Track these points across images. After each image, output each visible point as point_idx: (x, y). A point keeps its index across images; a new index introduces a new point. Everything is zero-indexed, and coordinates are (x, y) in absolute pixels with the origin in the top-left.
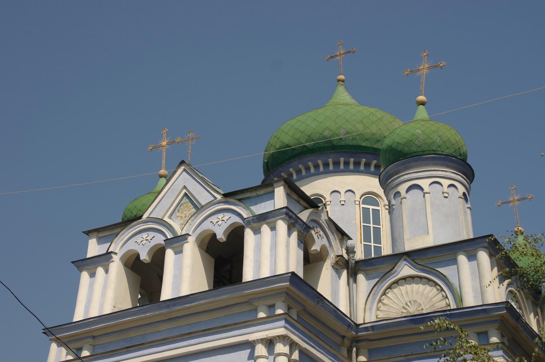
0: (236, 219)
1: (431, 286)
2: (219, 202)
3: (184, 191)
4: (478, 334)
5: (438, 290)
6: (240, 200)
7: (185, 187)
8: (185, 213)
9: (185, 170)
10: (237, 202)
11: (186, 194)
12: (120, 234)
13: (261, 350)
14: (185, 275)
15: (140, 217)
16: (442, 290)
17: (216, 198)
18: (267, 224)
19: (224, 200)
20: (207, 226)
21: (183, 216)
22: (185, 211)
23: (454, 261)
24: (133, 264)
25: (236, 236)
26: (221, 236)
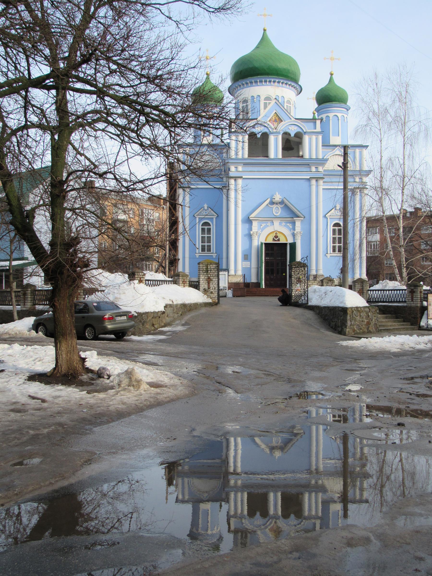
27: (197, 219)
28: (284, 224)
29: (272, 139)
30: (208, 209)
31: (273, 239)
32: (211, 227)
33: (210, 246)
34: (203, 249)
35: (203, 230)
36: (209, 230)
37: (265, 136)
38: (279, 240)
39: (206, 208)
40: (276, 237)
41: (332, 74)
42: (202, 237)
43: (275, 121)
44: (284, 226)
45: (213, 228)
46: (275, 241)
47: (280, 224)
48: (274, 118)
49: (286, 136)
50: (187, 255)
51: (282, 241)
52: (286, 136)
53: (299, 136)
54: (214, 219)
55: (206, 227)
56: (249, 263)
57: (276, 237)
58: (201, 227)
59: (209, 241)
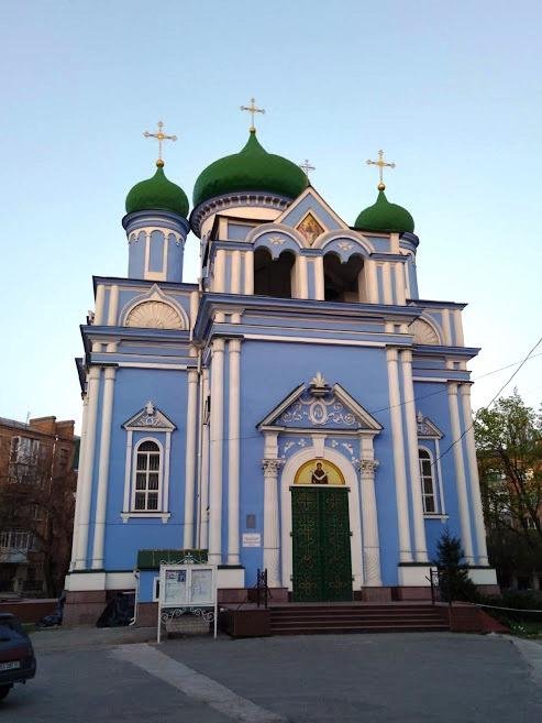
0: (359, 251)
14: (309, 281)
24: (261, 255)
25: (357, 261)
27: (130, 434)
28: (335, 443)
29: (301, 262)
30: (154, 414)
31: (313, 478)
32: (161, 453)
33: (156, 495)
34: (140, 503)
35: (142, 459)
36: (155, 460)
37: (288, 258)
38: (325, 481)
39: (150, 411)
40: (319, 473)
41: (382, 189)
42: (138, 475)
43: (309, 230)
44: (336, 448)
45: (164, 455)
46: (318, 482)
47: (327, 443)
48: (306, 224)
49: (331, 260)
50: (100, 516)
51: (334, 482)
53: (357, 261)
54: (168, 436)
55: (149, 453)
56: (258, 536)
57: (319, 473)
58: (136, 452)
59: (154, 485)
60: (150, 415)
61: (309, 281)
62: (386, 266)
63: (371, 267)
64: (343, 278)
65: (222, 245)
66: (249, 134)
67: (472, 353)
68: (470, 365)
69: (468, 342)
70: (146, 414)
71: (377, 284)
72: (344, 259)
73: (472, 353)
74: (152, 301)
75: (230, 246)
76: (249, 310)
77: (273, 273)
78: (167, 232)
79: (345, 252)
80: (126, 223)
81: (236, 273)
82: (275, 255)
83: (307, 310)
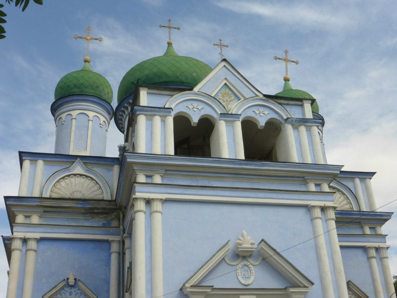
1: (340, 194)
2: (261, 99)
3: (225, 82)
4: (370, 228)
5: (345, 197)
6: (278, 103)
7: (226, 79)
8: (227, 98)
9: (225, 66)
10: (276, 104)
11: (225, 84)
12: (174, 96)
13: (317, 213)
14: (229, 143)
15: (191, 89)
16: (348, 198)
17: (257, 96)
18: (305, 126)
19: (264, 98)
20: (250, 113)
21: (225, 100)
22: (226, 96)
23: (354, 182)
24: (181, 122)
25: (274, 127)
26: (262, 122)
29: (222, 127)
37: (207, 125)
49: (249, 126)
52: (249, 126)
53: (274, 127)
60: (72, 286)
61: (229, 143)
62: (303, 129)
63: (289, 129)
64: (262, 143)
65: (142, 110)
66: (167, 45)
67: (382, 218)
68: (384, 229)
69: (380, 206)
70: (68, 285)
71: (297, 146)
72: (262, 122)
73: (382, 218)
74: (75, 175)
75: (151, 111)
76: (168, 170)
77: (194, 139)
78: (91, 114)
79: (262, 118)
80: (54, 109)
81: (156, 137)
82: (195, 119)
83: (231, 171)
